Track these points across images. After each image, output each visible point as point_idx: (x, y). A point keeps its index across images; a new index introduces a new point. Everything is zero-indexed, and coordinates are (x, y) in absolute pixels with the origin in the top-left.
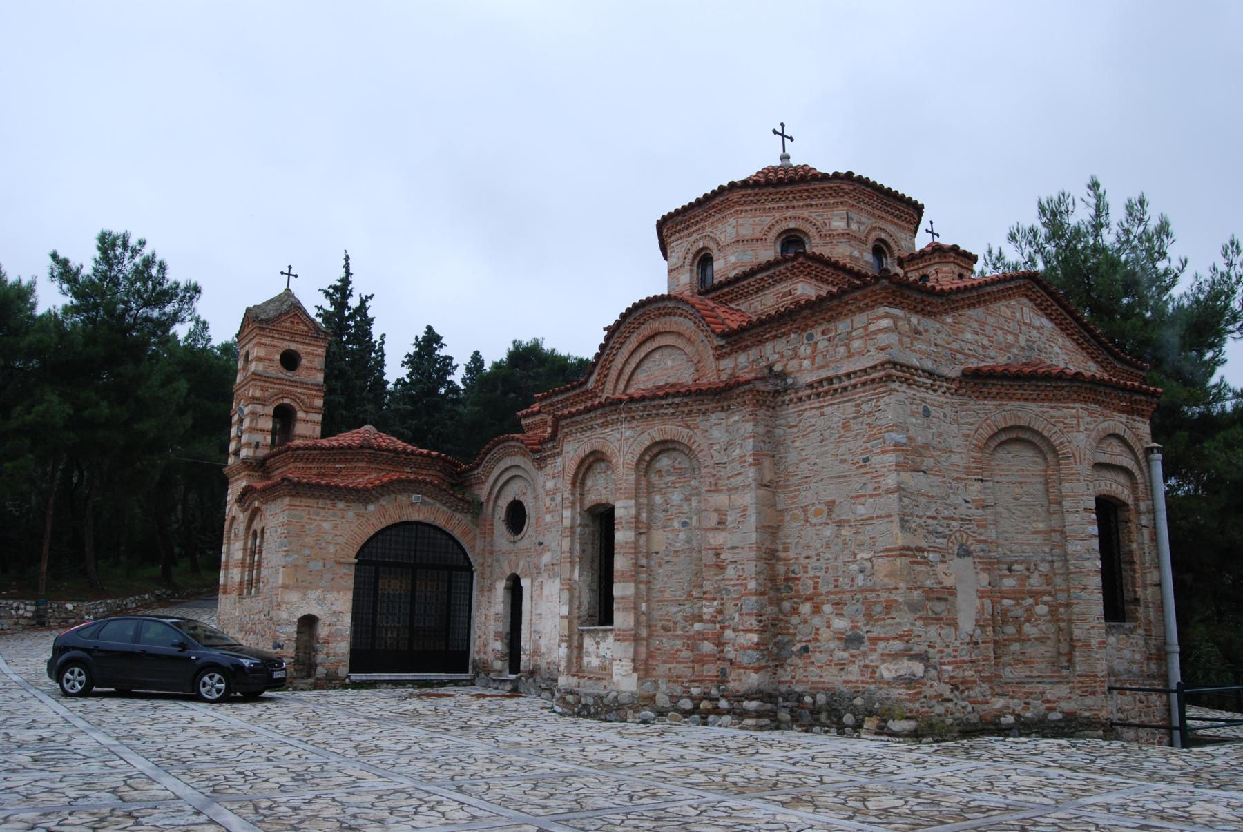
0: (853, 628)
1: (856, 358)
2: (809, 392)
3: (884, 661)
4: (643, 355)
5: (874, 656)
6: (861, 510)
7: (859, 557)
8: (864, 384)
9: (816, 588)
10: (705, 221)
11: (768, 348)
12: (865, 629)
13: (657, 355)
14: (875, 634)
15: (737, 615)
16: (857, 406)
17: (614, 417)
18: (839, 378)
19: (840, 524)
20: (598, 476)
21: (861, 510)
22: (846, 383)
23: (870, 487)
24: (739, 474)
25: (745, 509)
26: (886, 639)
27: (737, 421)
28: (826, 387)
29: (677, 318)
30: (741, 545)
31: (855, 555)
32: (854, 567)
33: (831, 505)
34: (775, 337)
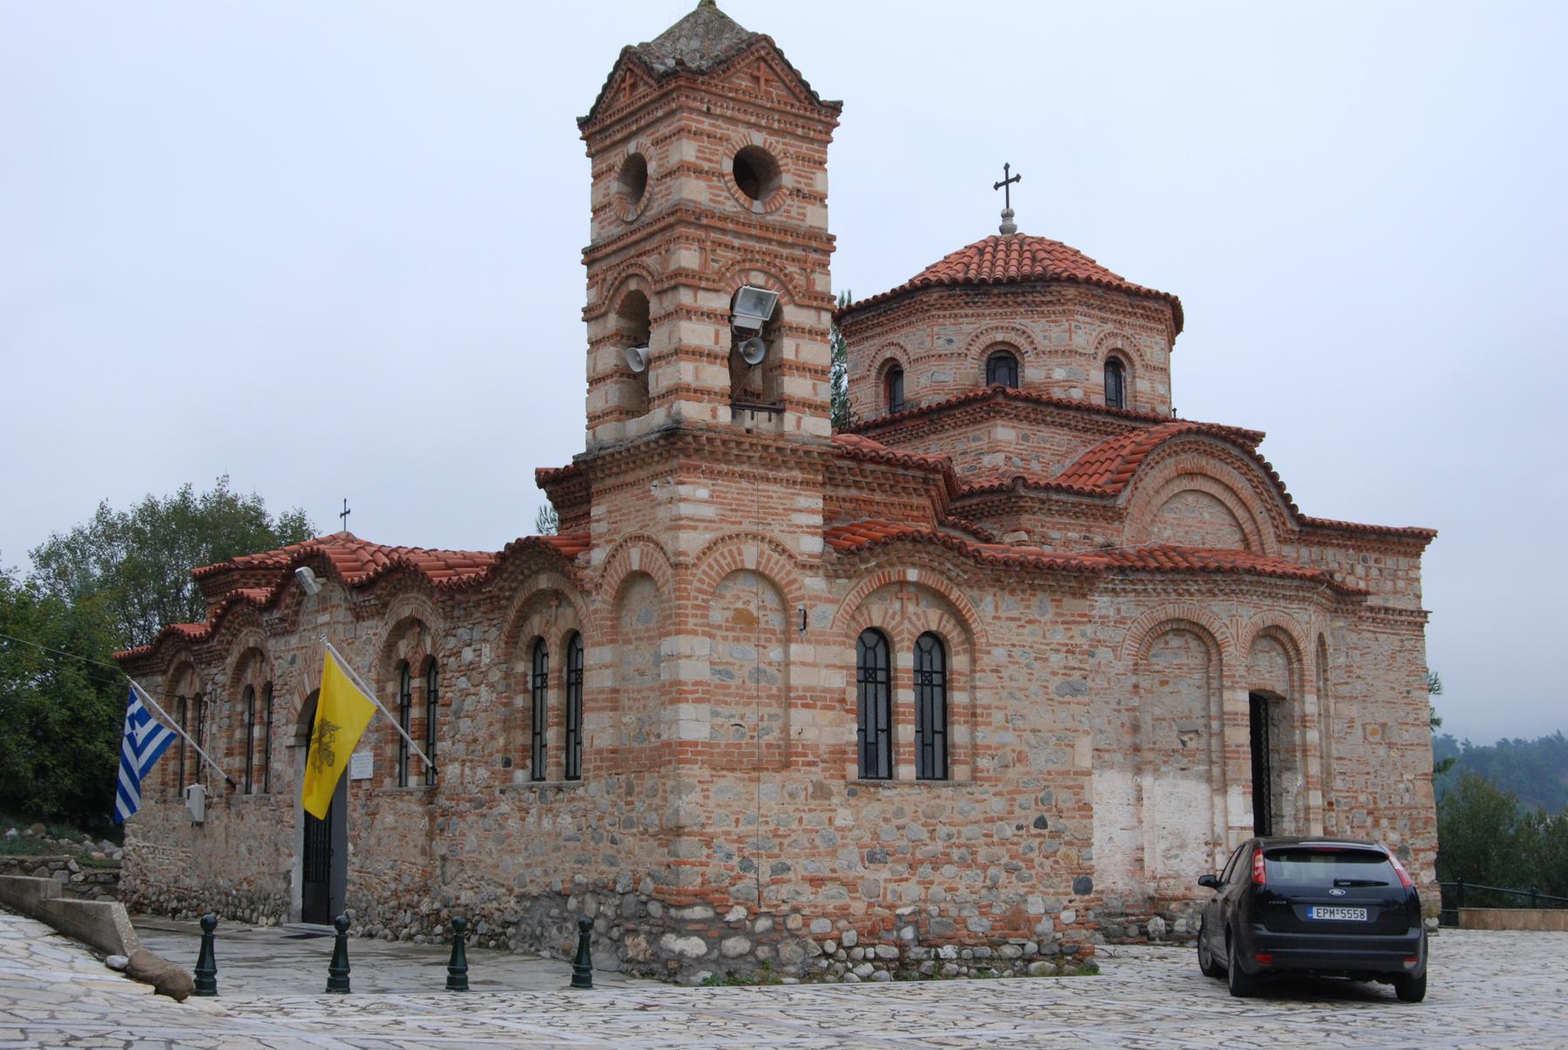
0: (1403, 840)
1: (1399, 596)
2: (1369, 614)
3: (1422, 869)
4: (1176, 491)
5: (1417, 865)
6: (1406, 736)
7: (1405, 777)
8: (1409, 623)
9: (1375, 803)
10: (1125, 316)
11: (1330, 553)
12: (1410, 842)
13: (1190, 499)
14: (1417, 846)
15: (1348, 827)
16: (1402, 641)
17: (1307, 595)
18: (1394, 610)
19: (1390, 745)
20: (1260, 655)
21: (1406, 736)
22: (1398, 618)
23: (1412, 716)
24: (1347, 683)
25: (1352, 721)
26: (1423, 850)
27: (1341, 628)
28: (1382, 616)
29: (1230, 468)
30: (1348, 756)
31: (1402, 775)
32: (1402, 786)
33: (1384, 725)
34: (1338, 545)
